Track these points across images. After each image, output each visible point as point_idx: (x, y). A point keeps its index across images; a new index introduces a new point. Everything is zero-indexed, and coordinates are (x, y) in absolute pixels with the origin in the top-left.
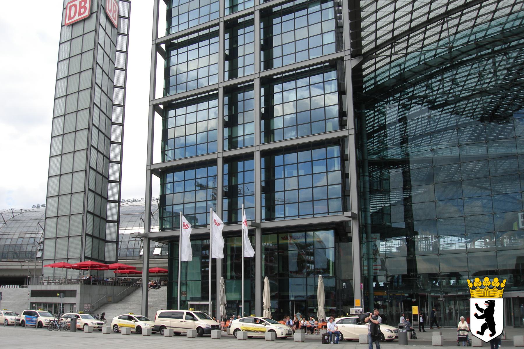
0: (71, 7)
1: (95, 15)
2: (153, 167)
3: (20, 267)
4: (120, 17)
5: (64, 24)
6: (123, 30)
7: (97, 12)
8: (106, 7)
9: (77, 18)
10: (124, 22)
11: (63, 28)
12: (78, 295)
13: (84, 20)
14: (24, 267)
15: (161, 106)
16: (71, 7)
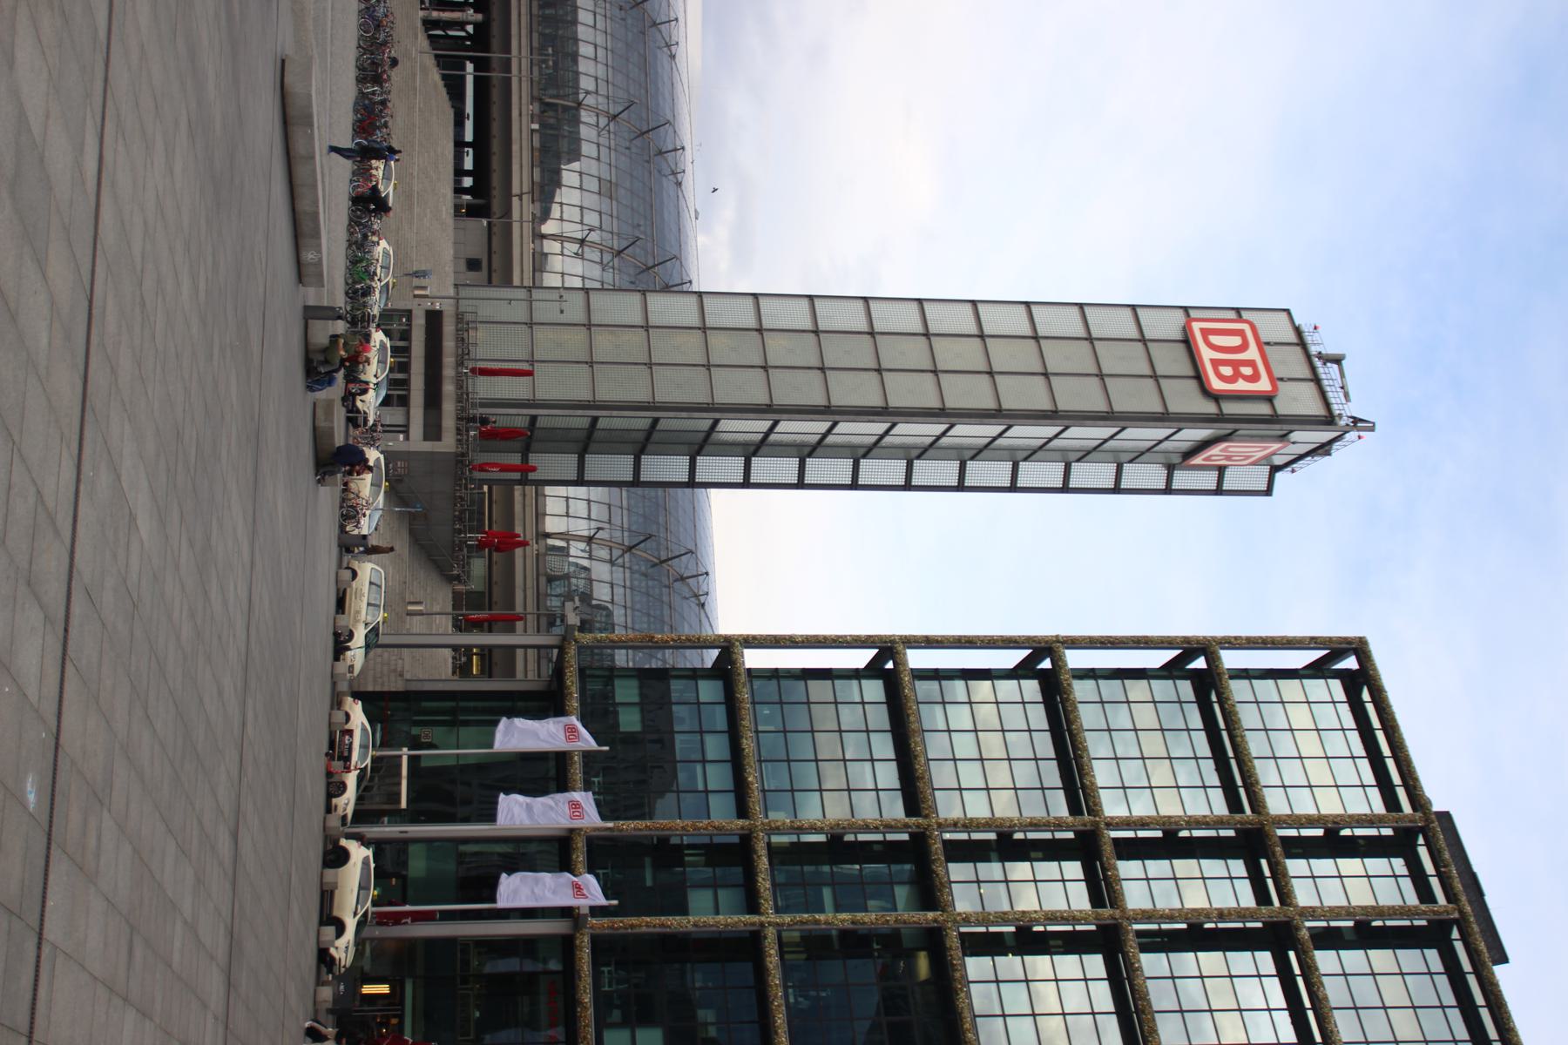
0: (1241, 333)
1: (1210, 408)
2: (738, 647)
3: (515, 190)
4: (1221, 470)
5: (1193, 314)
6: (1182, 479)
7: (1220, 418)
8: (1232, 441)
9: (1207, 354)
10: (1209, 479)
11: (1181, 313)
12: (428, 446)
13: (1199, 377)
14: (515, 200)
15: (890, 665)
16: (1241, 333)
